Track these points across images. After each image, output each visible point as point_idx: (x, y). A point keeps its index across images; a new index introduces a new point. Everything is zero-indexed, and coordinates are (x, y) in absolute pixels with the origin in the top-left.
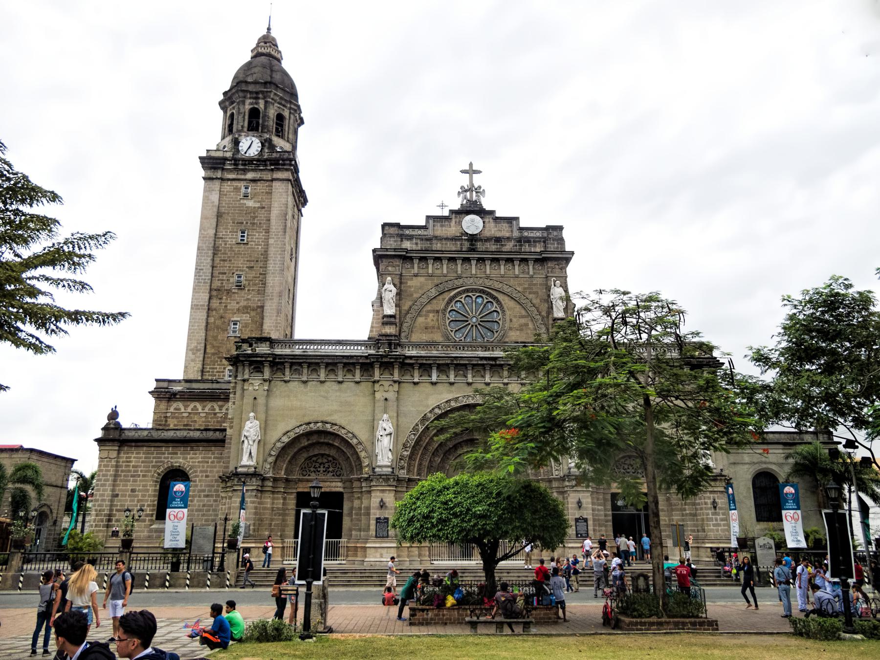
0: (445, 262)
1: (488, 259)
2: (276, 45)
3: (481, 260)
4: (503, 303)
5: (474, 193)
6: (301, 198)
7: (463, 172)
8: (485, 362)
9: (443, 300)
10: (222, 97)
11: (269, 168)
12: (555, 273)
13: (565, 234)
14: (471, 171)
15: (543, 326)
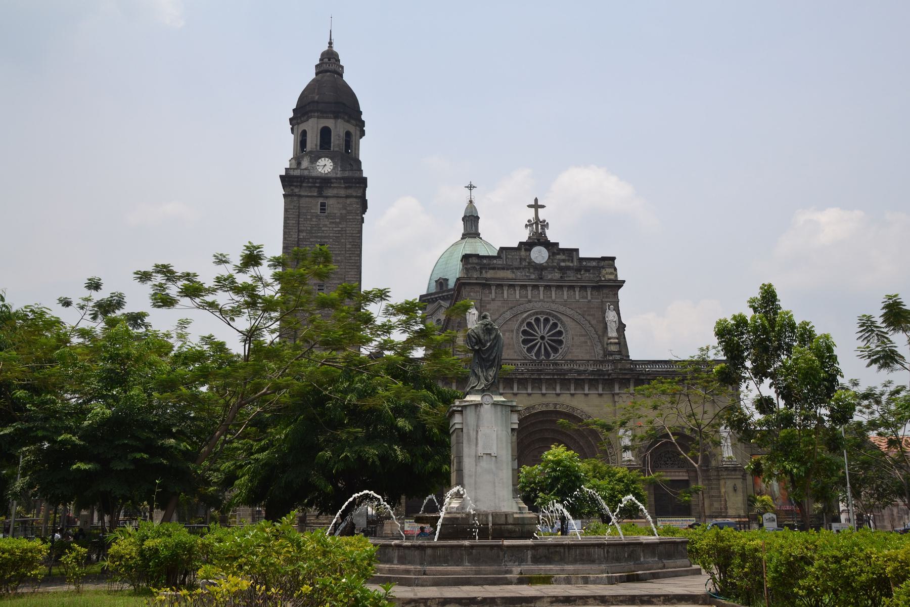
0: (518, 289)
1: (553, 286)
2: (339, 61)
3: (548, 287)
4: (566, 323)
5: (539, 226)
6: (364, 207)
7: (530, 206)
8: (556, 377)
9: (517, 321)
10: (291, 115)
11: (343, 186)
12: (609, 298)
13: (617, 264)
14: (536, 206)
15: (599, 344)
